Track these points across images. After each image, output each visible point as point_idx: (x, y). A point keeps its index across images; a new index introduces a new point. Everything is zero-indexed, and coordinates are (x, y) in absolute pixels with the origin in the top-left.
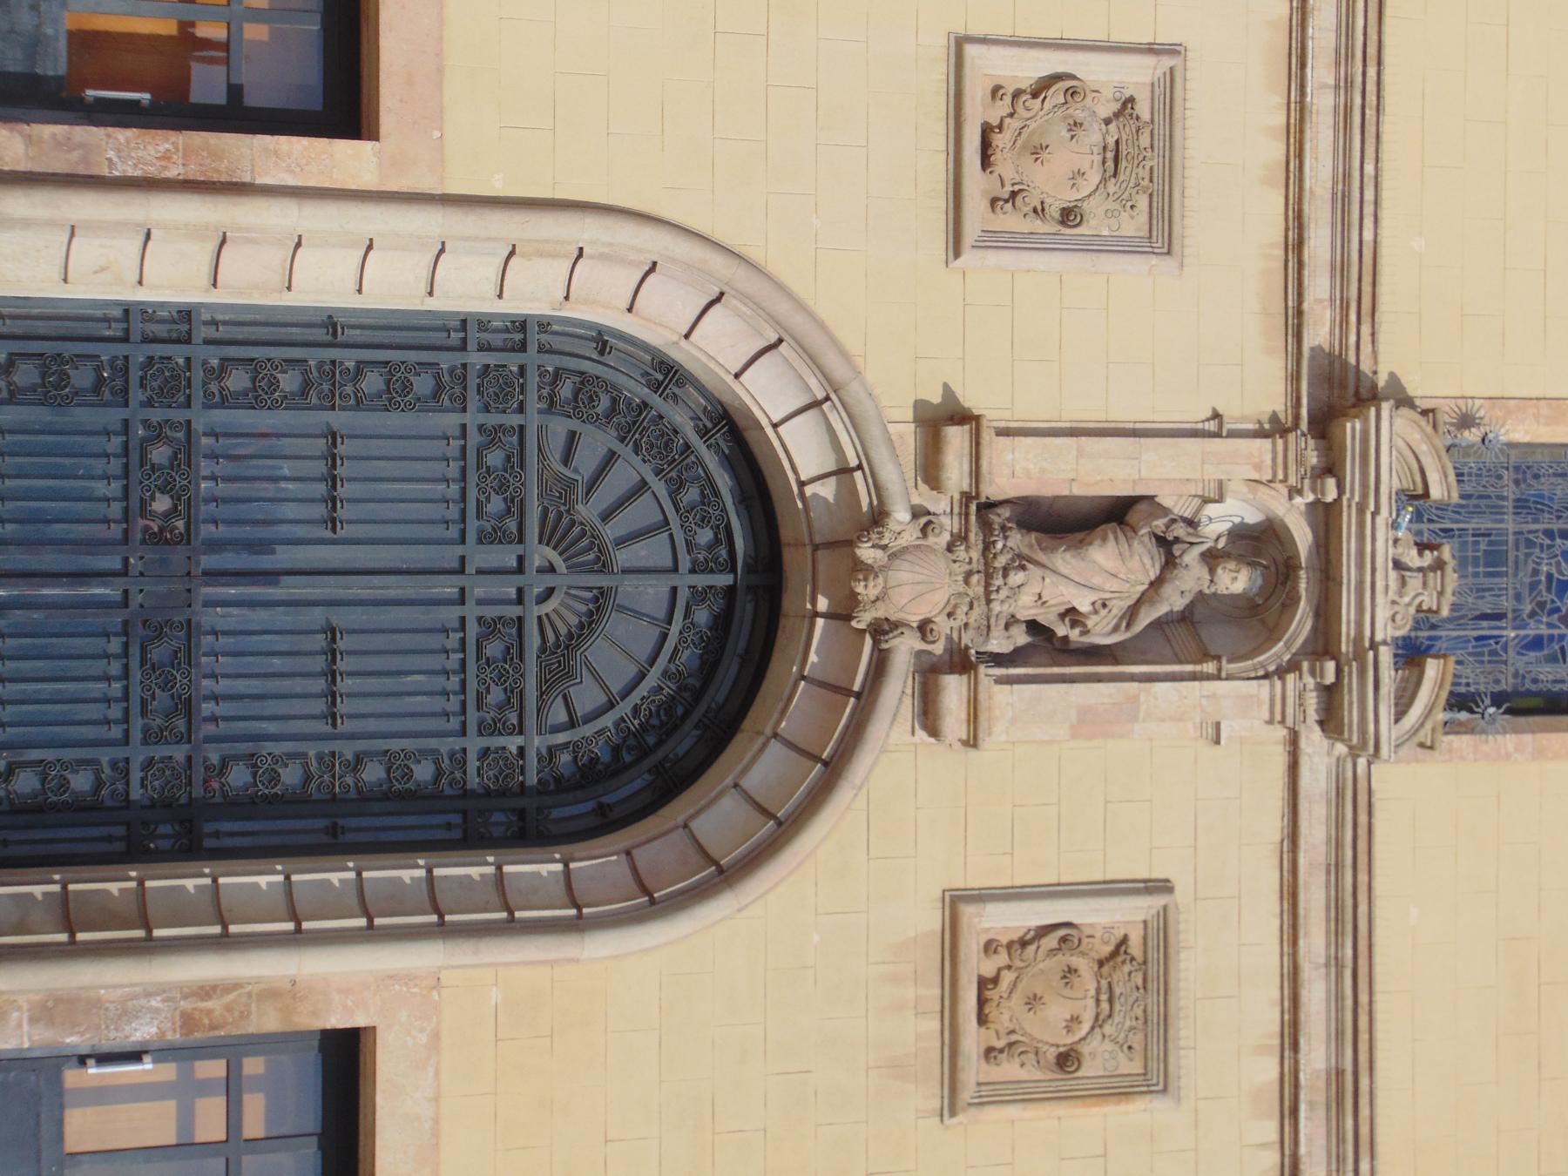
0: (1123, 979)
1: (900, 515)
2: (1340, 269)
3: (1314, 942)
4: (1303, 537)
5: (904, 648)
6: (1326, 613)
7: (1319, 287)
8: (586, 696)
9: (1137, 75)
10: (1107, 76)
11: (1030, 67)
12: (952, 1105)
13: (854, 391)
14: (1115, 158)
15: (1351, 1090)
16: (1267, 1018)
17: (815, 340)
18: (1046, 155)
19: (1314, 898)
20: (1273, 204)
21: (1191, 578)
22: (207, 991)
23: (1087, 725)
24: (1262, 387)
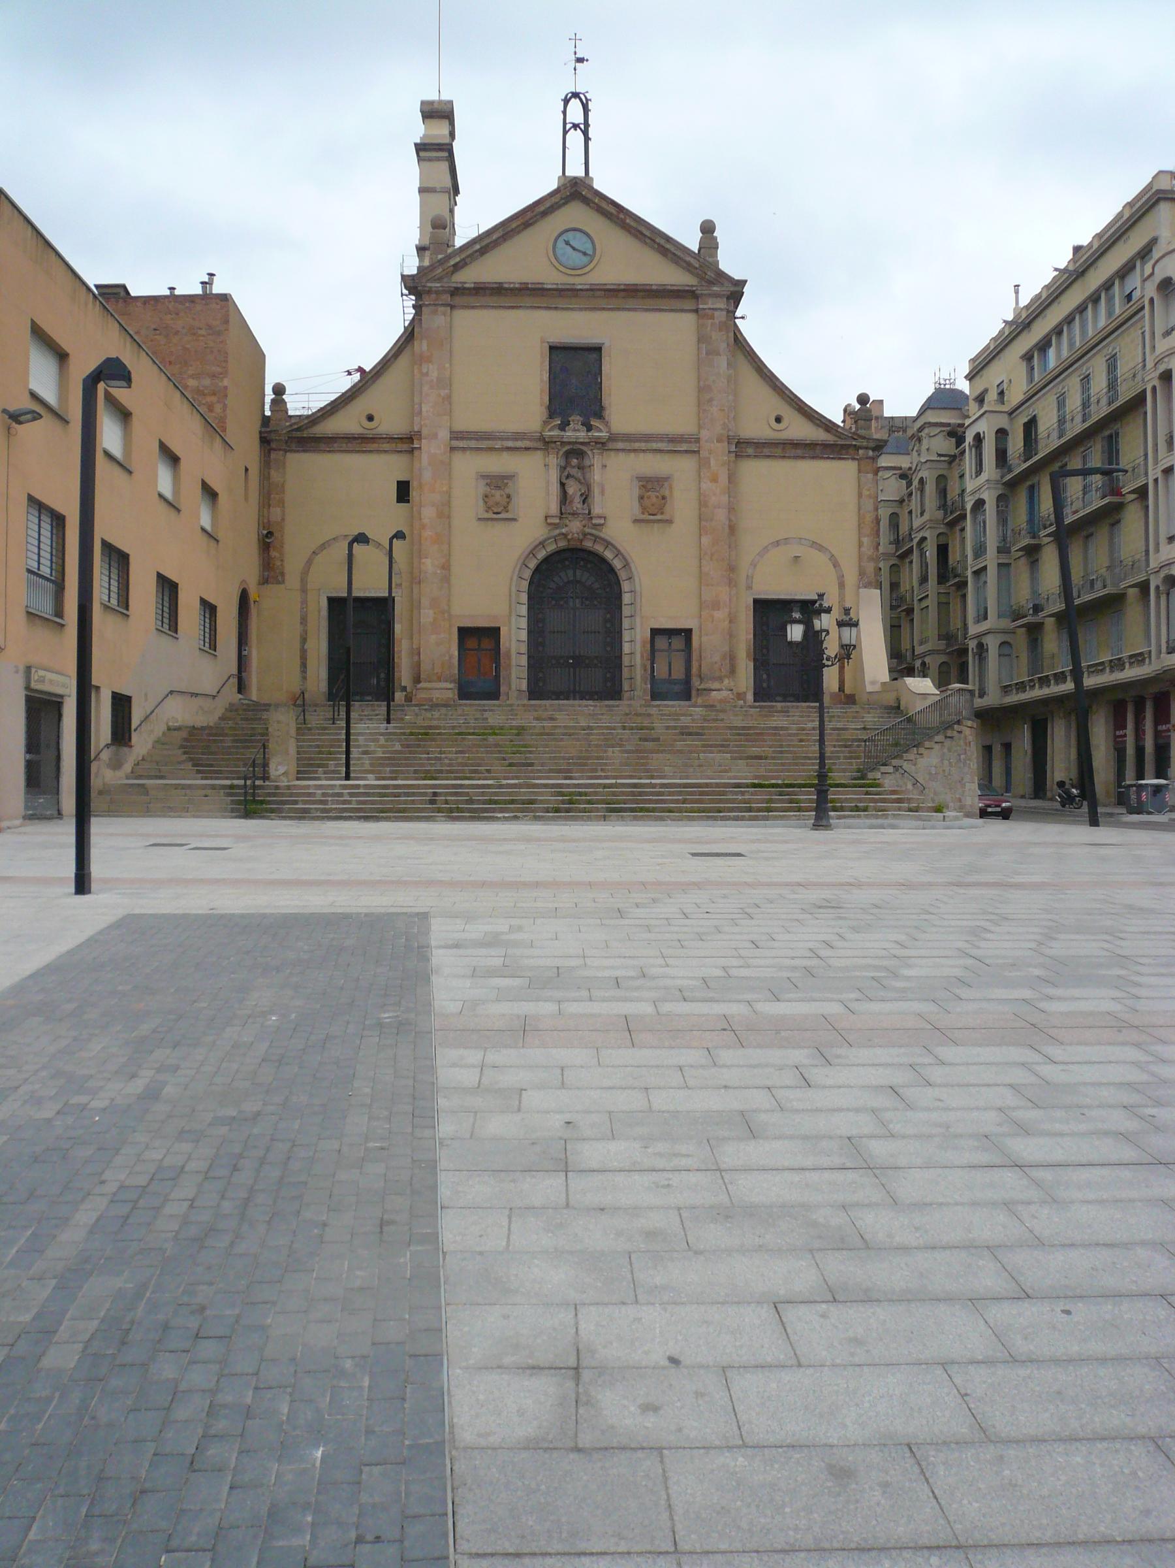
0: (649, 486)
1: (564, 531)
2: (516, 440)
3: (643, 445)
4: (566, 448)
5: (587, 530)
6: (582, 443)
7: (519, 444)
8: (596, 585)
9: (482, 483)
10: (482, 489)
11: (481, 503)
12: (669, 522)
13: (542, 538)
14: (498, 487)
15: (673, 439)
16: (658, 456)
17: (532, 546)
18: (498, 499)
19: (637, 445)
20: (505, 454)
21: (574, 472)
22: (642, 656)
23: (602, 493)
24: (539, 454)
